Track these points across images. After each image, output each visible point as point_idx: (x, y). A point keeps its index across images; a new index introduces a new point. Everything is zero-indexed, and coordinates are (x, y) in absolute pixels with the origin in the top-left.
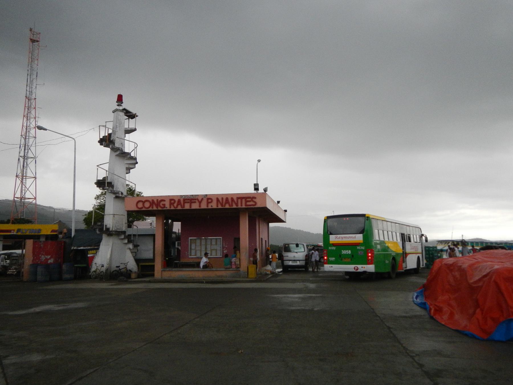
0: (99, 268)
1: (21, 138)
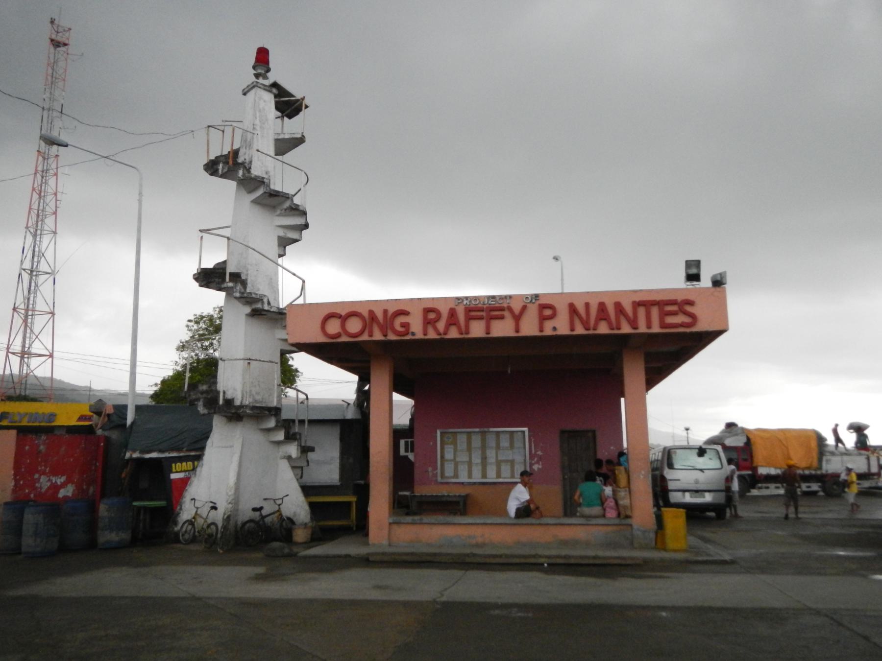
0: (204, 512)
1: (26, 232)
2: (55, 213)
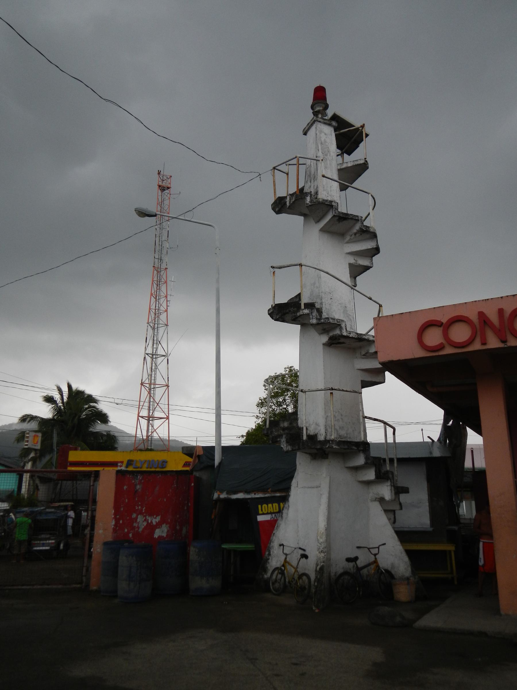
0: (294, 559)
1: (148, 326)
2: (166, 311)
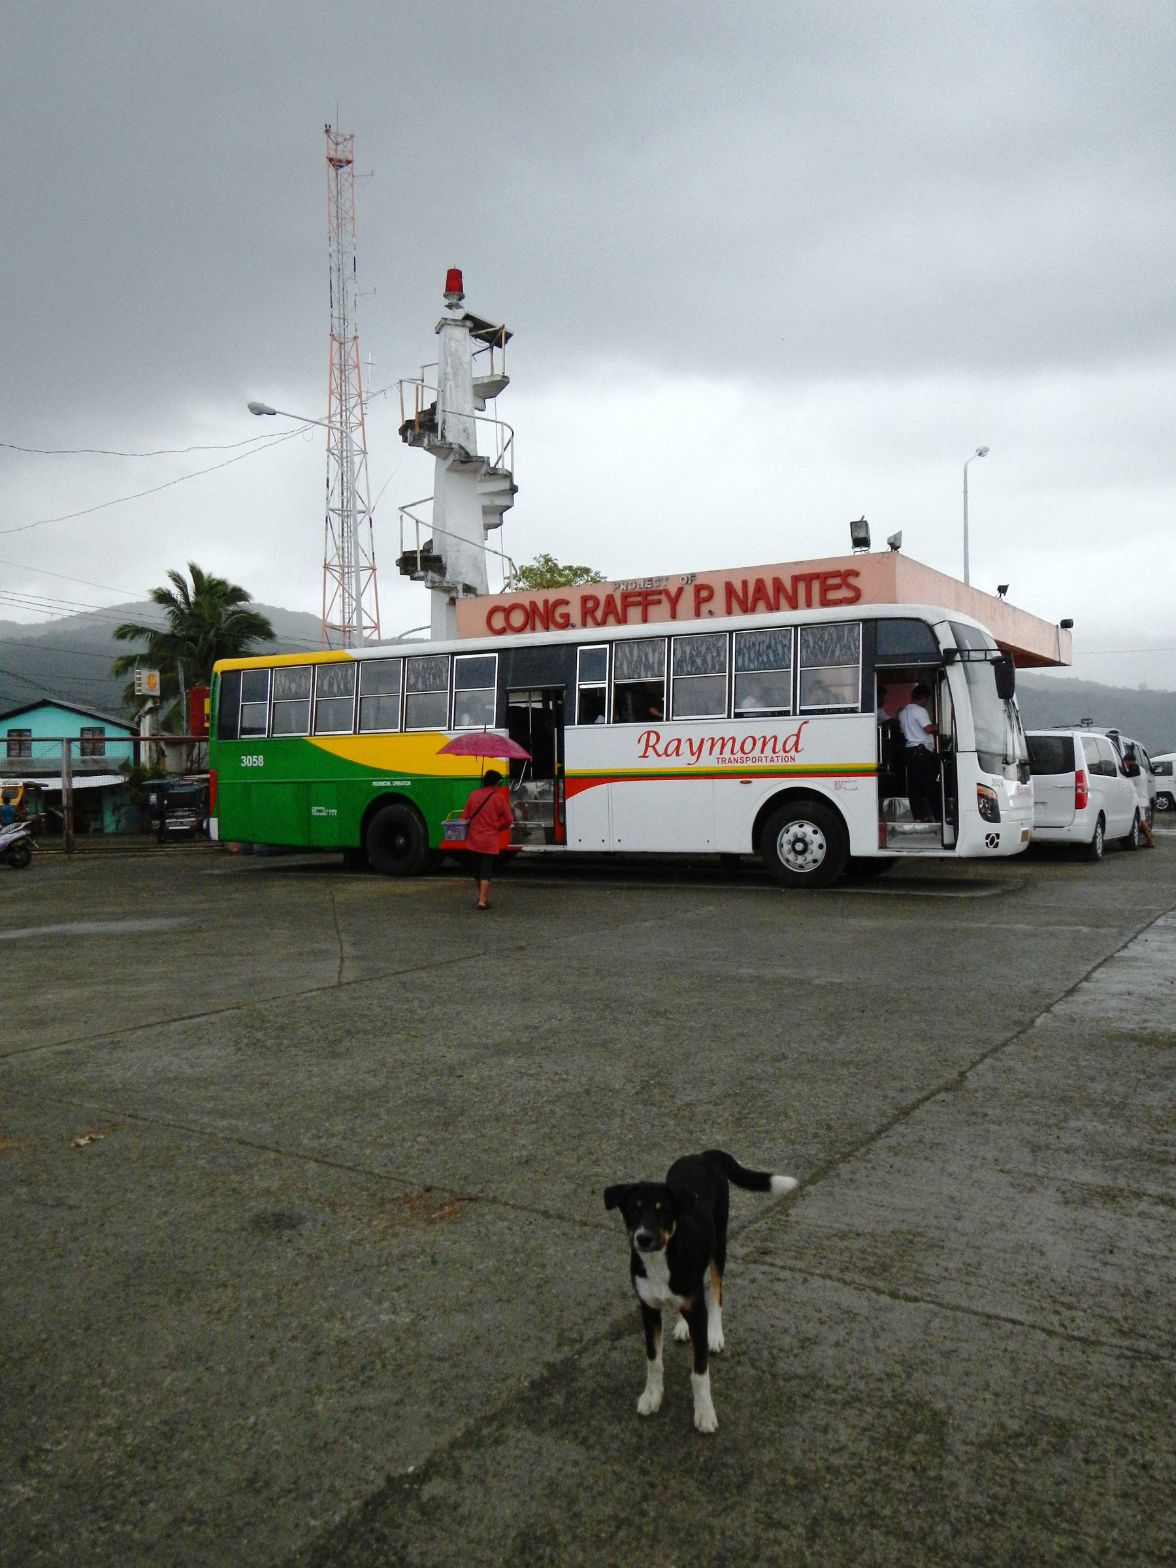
2: (362, 424)
